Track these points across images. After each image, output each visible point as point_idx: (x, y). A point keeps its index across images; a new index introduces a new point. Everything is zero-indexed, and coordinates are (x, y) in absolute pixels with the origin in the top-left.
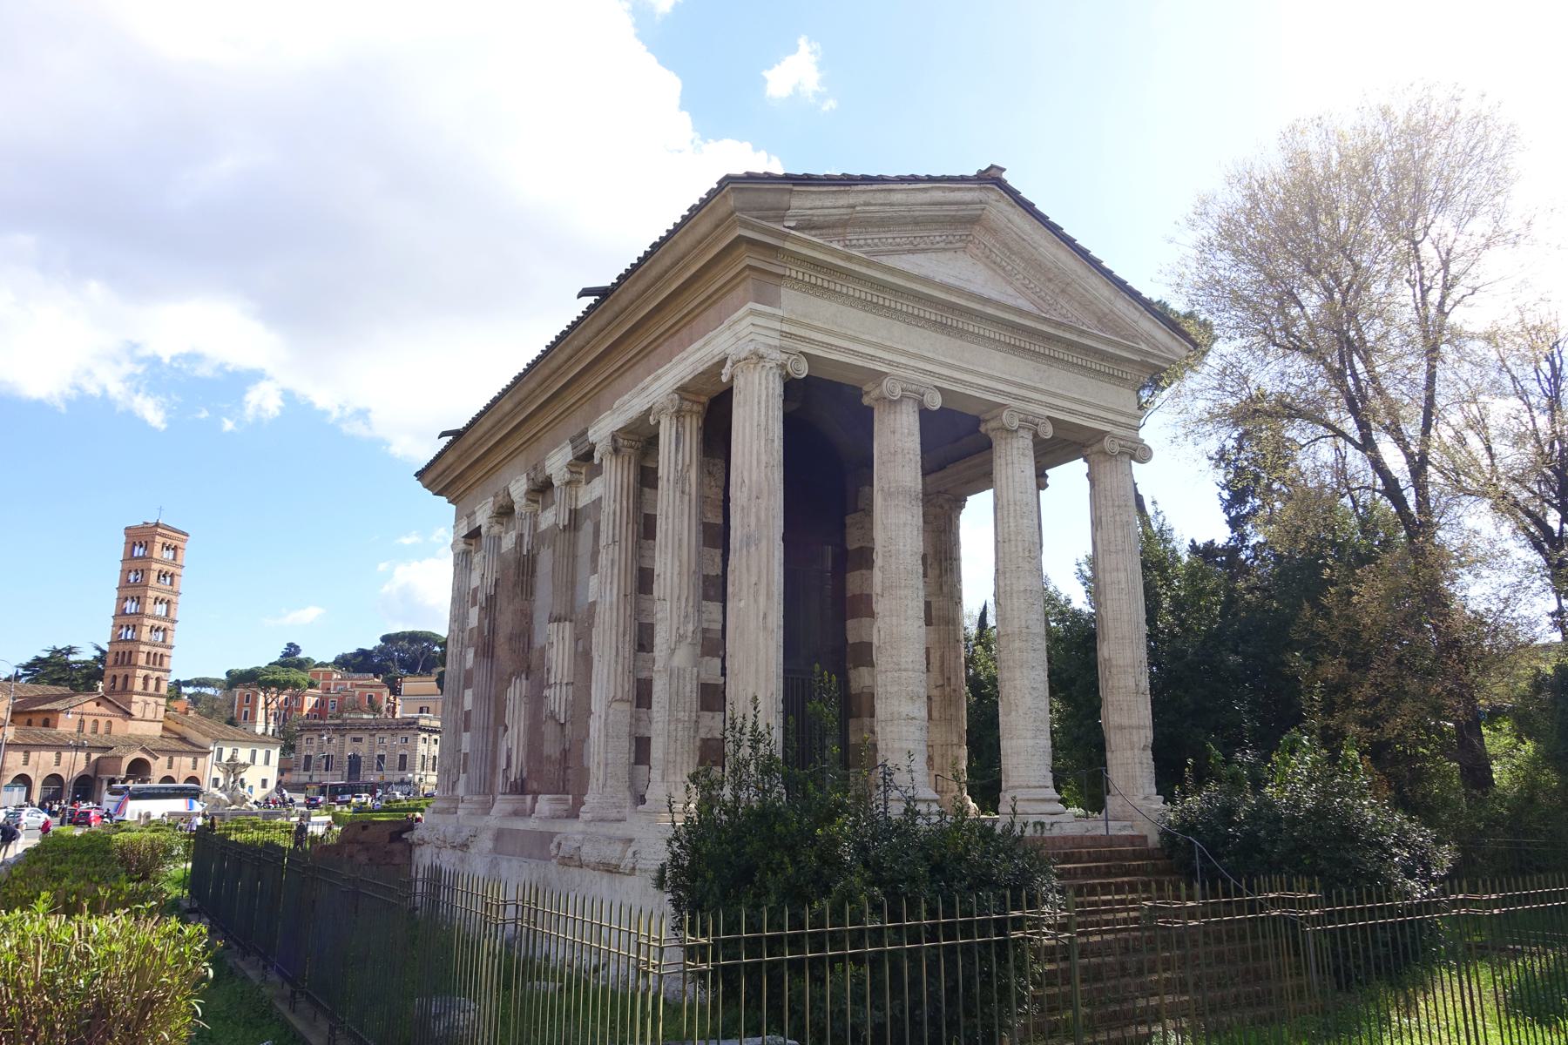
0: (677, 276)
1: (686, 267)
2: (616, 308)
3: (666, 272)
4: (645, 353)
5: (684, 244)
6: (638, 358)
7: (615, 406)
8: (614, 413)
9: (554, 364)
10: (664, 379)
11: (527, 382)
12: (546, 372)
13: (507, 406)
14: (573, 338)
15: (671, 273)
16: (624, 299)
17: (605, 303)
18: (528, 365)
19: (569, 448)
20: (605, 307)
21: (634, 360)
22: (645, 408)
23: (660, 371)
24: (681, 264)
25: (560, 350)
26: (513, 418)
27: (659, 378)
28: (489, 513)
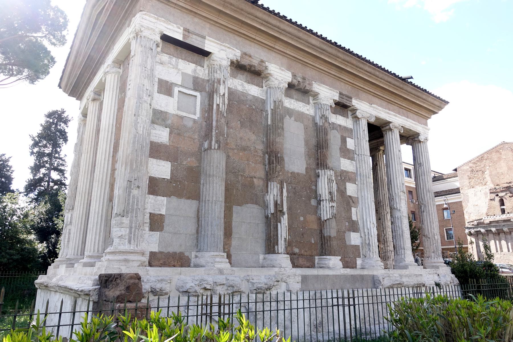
0: (421, 101)
1: (424, 103)
2: (401, 86)
3: (421, 98)
4: (389, 102)
5: (430, 99)
6: (386, 100)
7: (373, 105)
8: (371, 107)
9: (361, 65)
10: (397, 118)
11: (339, 51)
12: (354, 62)
13: (314, 41)
14: (379, 71)
15: (421, 100)
16: (405, 87)
17: (400, 80)
18: (349, 49)
19: (338, 95)
20: (399, 81)
21: (383, 99)
22: (388, 119)
23: (398, 115)
24: (424, 101)
25: (369, 66)
26: (309, 47)
27: (396, 116)
28: (232, 57)
